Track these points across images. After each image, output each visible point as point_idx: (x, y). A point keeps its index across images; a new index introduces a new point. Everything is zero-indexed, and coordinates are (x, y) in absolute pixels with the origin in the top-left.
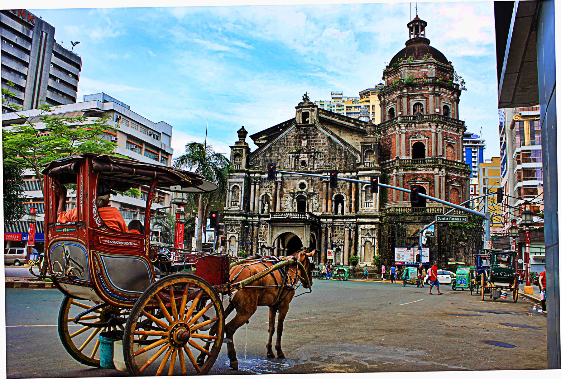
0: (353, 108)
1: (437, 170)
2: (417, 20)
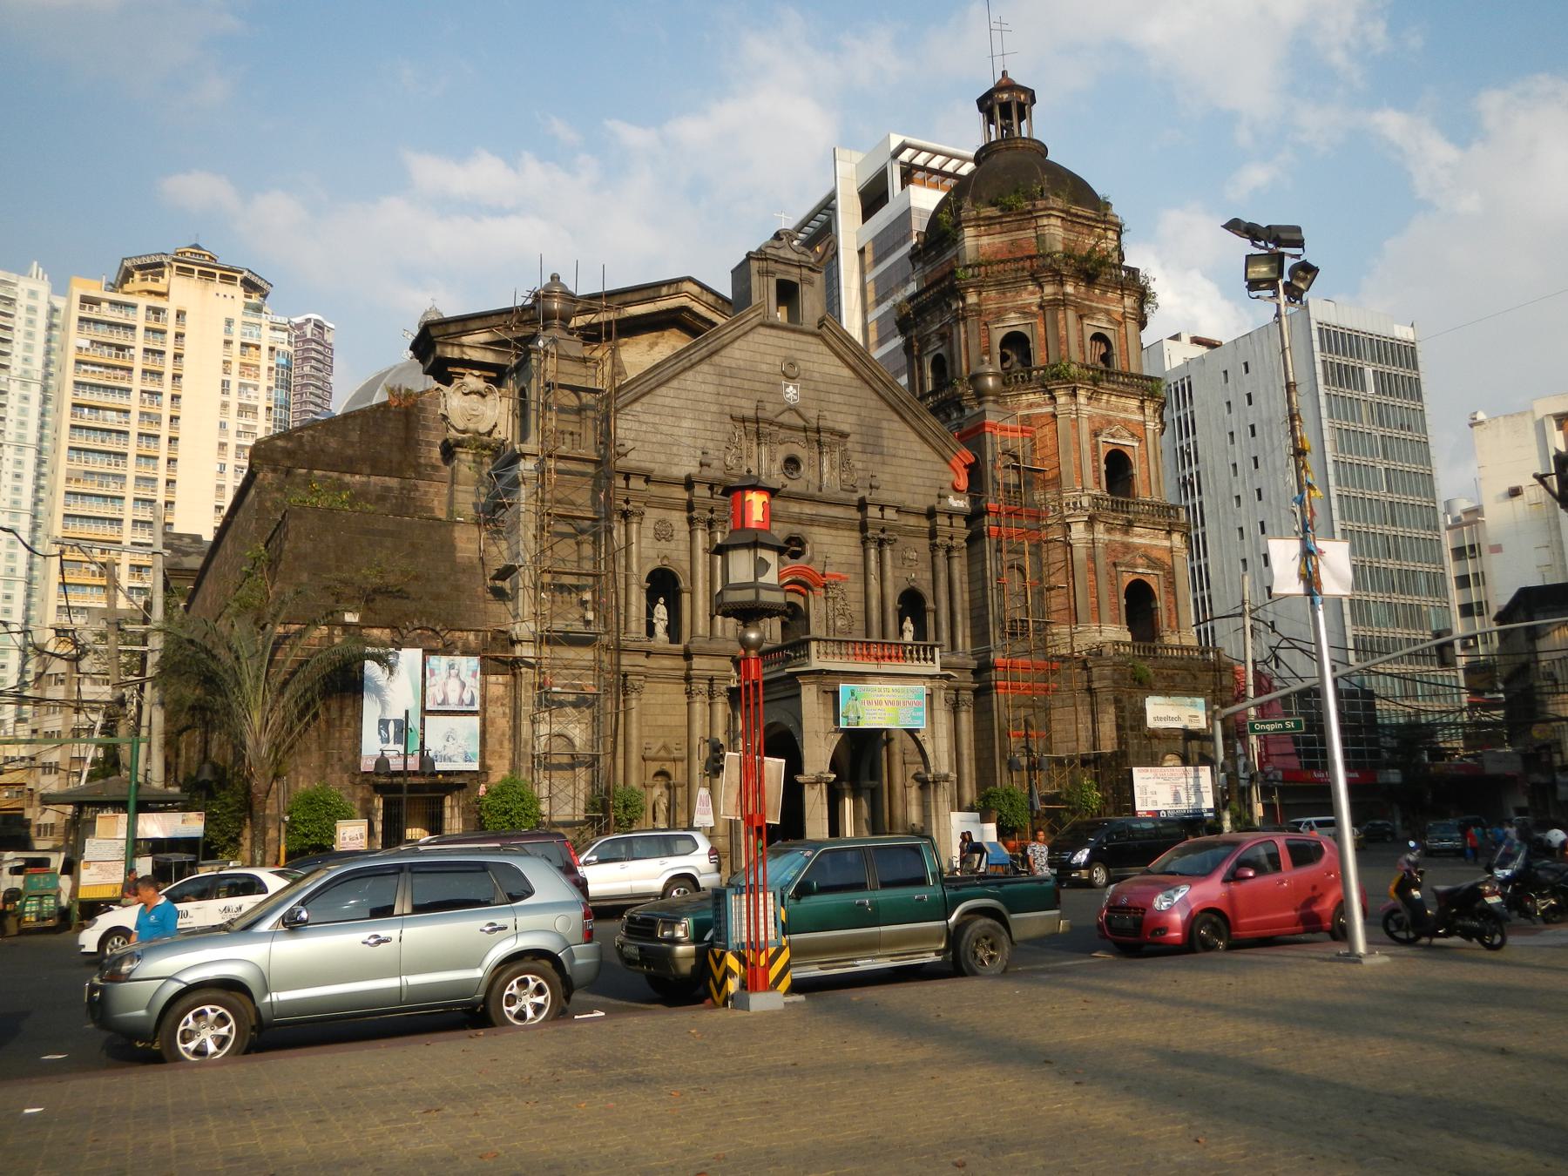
0: (105, 305)
1: (1176, 537)
2: (1006, 85)
